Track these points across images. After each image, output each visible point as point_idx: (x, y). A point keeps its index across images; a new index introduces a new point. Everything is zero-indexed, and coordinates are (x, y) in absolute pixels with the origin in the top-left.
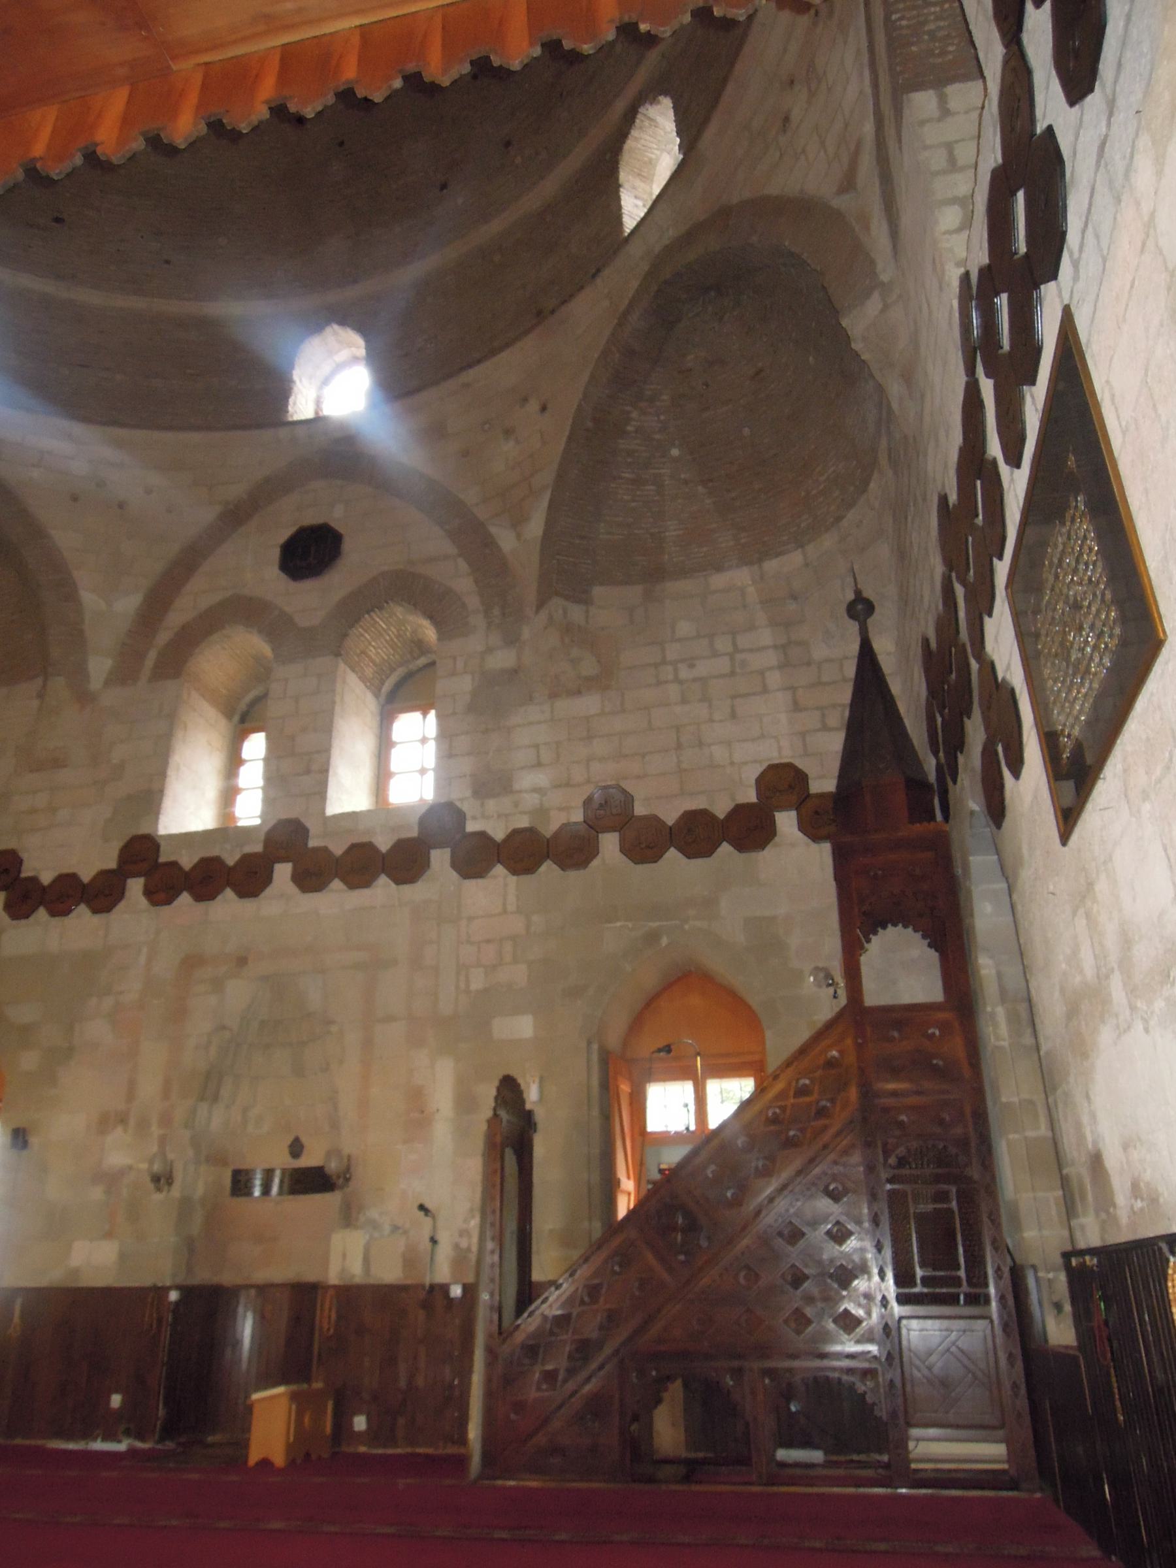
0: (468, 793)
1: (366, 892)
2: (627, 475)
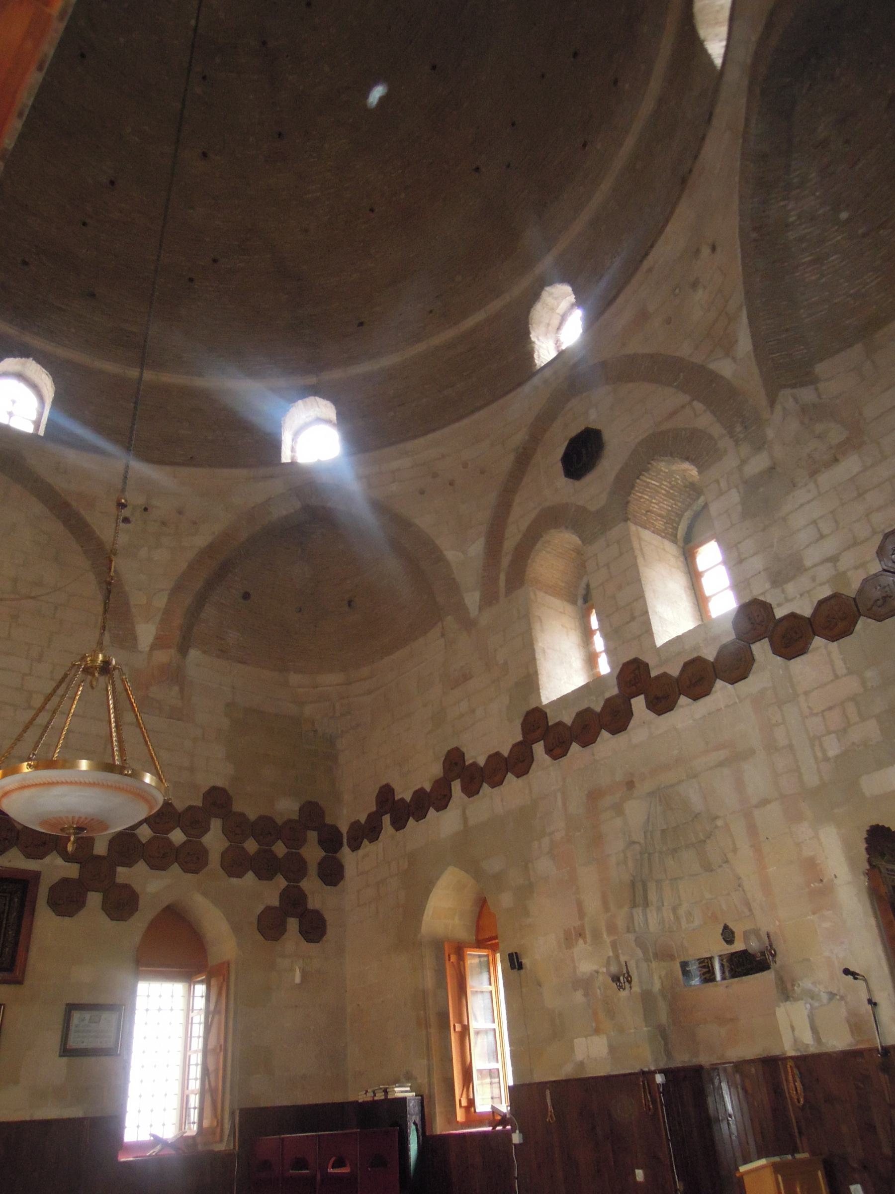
0: (767, 586)
1: (707, 699)
2: (806, 259)
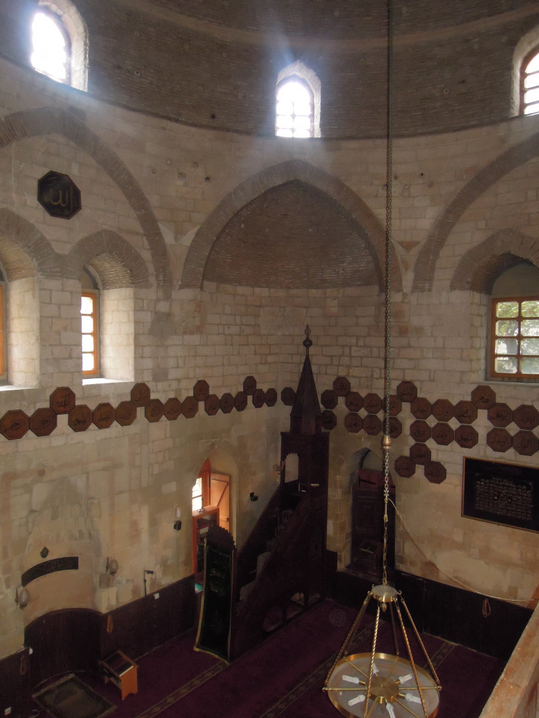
1: (107, 430)
